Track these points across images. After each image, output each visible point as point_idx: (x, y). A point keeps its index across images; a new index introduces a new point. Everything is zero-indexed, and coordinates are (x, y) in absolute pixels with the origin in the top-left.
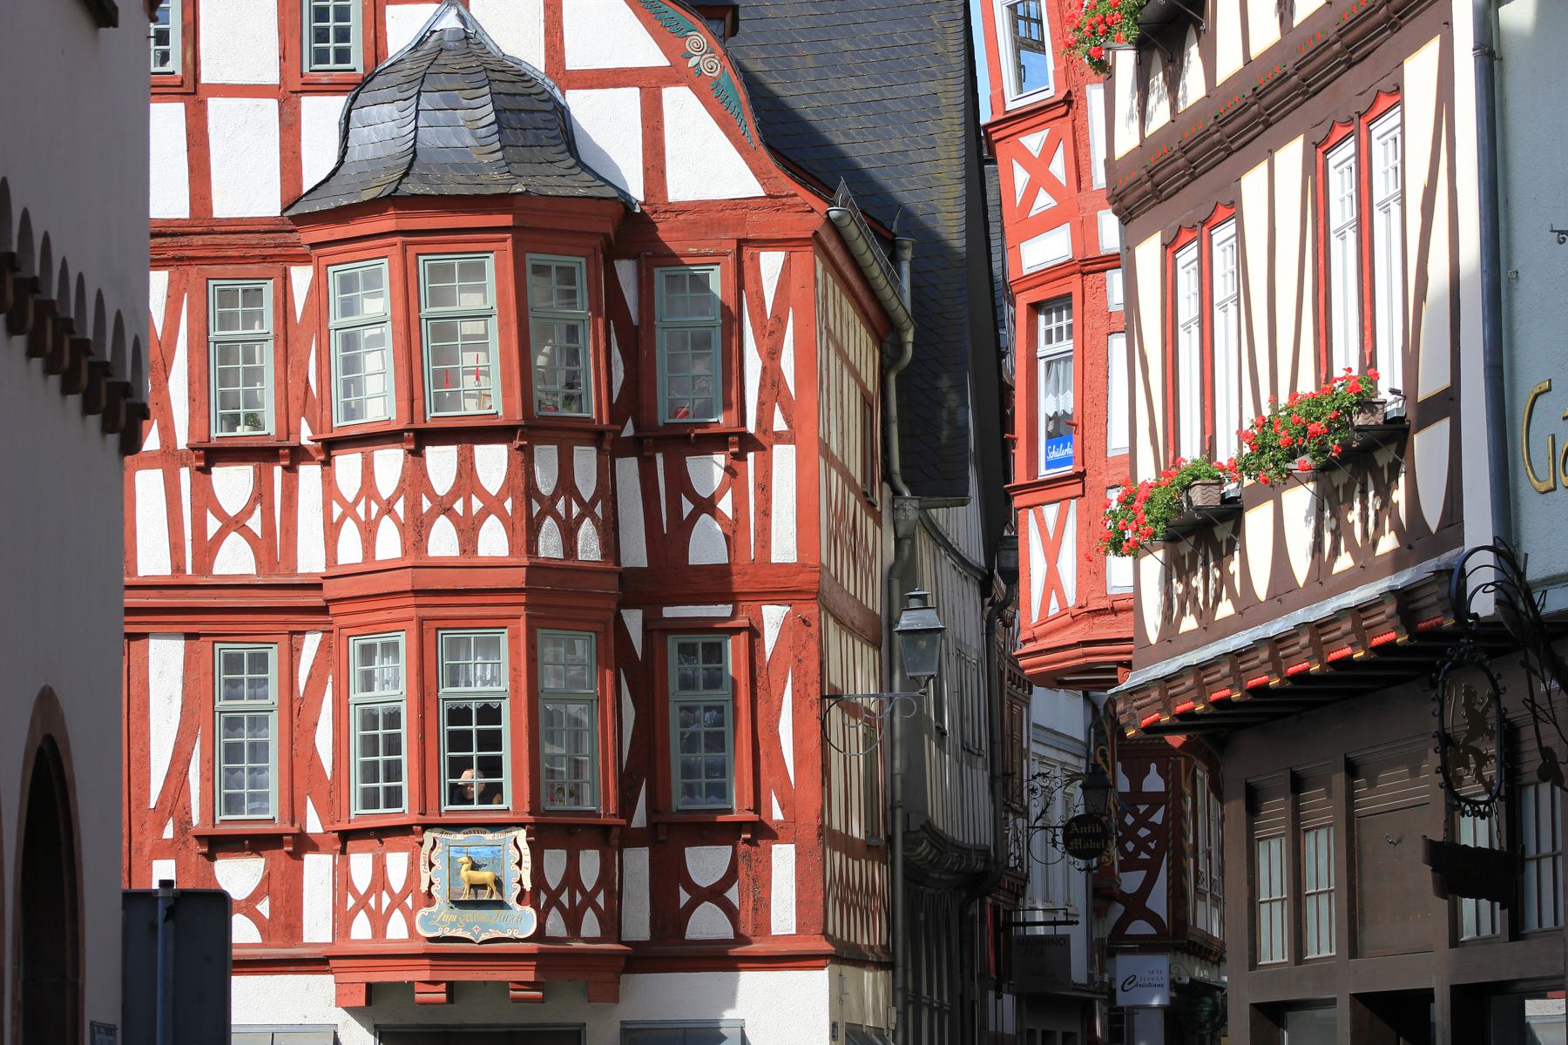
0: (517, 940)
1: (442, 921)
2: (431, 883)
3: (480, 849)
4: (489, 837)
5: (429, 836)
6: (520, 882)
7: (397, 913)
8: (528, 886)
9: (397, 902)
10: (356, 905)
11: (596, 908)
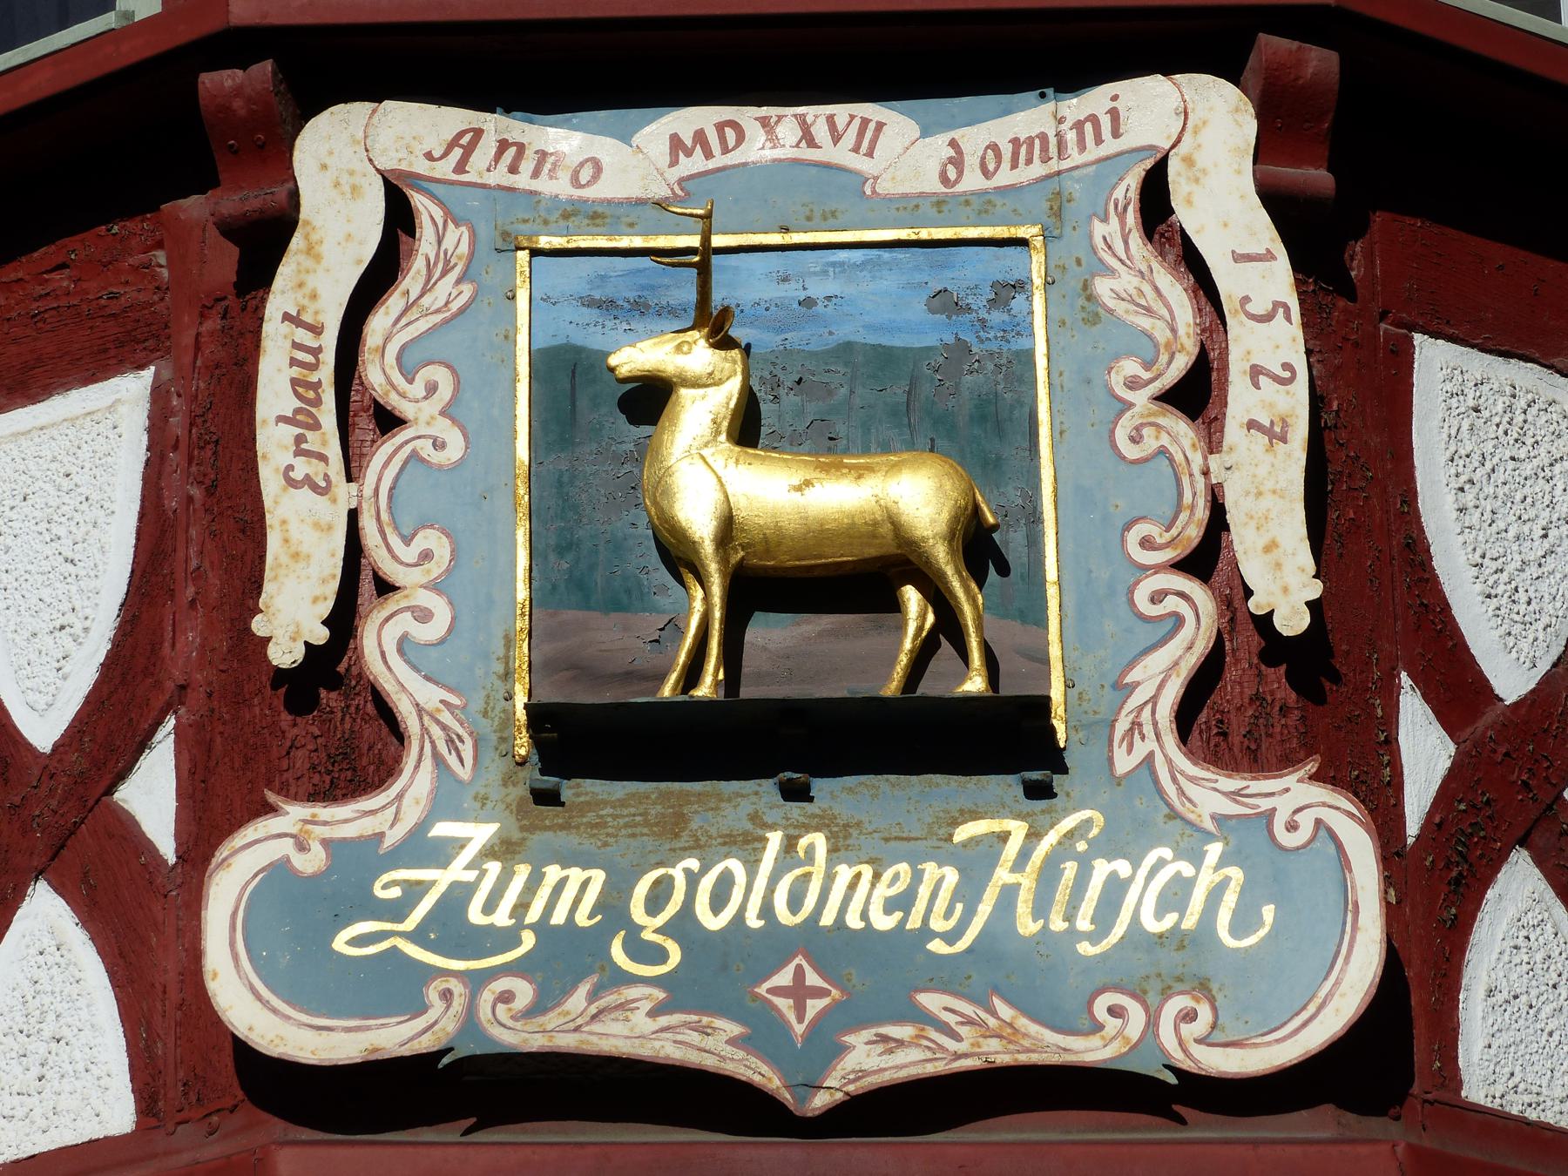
2: (358, 585)
5: (342, 160)
8: (1283, 579)
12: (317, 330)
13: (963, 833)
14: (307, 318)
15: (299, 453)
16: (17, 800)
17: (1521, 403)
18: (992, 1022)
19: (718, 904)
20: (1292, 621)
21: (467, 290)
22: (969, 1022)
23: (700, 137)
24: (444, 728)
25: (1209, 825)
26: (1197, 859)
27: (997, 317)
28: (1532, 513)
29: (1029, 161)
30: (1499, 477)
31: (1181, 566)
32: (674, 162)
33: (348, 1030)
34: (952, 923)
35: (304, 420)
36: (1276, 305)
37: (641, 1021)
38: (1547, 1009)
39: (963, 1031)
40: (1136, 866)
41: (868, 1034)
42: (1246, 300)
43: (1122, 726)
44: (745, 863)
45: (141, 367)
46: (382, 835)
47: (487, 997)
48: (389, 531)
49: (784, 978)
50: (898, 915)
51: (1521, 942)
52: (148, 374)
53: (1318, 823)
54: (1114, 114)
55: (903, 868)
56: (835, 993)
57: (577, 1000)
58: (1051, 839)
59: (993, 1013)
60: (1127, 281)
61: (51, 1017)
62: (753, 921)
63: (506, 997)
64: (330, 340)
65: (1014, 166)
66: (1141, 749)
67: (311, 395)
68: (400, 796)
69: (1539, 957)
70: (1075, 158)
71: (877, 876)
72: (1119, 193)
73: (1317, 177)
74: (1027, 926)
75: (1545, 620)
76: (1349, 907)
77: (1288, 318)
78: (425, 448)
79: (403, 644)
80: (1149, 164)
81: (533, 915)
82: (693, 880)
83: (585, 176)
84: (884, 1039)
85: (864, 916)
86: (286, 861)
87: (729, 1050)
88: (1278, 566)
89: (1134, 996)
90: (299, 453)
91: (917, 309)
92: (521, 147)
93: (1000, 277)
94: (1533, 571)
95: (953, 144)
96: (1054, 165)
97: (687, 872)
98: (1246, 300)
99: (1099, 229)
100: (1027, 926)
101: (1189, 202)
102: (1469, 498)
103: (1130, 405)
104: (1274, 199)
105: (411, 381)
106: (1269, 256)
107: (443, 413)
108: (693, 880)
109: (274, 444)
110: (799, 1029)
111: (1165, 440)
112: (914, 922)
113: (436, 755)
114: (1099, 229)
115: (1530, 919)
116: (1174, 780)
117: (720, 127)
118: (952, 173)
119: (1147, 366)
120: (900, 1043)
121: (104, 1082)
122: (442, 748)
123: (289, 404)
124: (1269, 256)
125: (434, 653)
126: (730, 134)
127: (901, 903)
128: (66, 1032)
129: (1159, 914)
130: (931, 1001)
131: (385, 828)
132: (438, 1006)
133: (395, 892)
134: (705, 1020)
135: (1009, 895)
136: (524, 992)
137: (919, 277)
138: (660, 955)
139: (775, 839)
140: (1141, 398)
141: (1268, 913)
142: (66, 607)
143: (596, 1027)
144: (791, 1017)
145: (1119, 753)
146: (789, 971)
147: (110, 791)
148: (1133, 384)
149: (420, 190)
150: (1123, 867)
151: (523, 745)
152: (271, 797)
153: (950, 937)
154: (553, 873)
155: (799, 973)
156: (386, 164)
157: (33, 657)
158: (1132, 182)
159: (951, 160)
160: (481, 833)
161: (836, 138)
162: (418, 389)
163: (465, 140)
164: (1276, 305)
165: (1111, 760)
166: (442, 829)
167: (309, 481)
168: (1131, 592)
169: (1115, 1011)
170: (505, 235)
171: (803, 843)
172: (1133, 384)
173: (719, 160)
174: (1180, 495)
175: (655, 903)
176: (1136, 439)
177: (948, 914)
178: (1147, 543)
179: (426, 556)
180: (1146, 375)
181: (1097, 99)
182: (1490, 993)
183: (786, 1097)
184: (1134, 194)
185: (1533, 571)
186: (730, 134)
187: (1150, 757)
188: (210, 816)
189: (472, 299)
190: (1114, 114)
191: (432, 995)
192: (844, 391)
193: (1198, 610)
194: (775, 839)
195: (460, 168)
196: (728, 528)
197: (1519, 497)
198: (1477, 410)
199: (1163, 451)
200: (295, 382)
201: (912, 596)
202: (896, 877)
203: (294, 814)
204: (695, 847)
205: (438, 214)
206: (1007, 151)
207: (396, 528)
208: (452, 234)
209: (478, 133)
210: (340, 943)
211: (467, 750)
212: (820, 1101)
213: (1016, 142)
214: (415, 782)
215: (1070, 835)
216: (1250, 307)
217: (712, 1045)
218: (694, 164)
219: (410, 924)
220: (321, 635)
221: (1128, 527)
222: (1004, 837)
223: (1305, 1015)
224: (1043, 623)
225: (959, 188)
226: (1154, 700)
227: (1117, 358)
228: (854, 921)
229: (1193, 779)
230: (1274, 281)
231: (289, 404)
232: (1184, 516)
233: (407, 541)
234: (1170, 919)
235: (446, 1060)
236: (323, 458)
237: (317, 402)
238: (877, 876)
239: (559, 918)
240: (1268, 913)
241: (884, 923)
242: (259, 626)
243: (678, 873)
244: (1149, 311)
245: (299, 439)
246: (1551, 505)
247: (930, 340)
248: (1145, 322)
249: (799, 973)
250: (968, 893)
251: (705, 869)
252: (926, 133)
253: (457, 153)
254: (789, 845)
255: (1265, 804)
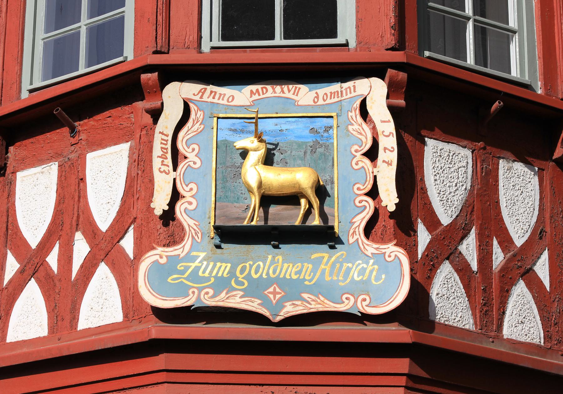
0: (364, 318)
1: (195, 272)
2: (176, 196)
3: (284, 125)
4: (305, 95)
6: (373, 193)
7: (103, 271)
8: (390, 198)
9: (105, 248)
10: (21, 272)
11: (534, 284)
12: (167, 136)
13: (313, 257)
14: (165, 133)
15: (162, 165)
16: (97, 243)
17: (451, 154)
18: (319, 301)
19: (256, 273)
20: (392, 208)
21: (202, 126)
22: (313, 301)
23: (257, 90)
24: (195, 230)
25: (370, 255)
26: (367, 263)
27: (326, 134)
28: (453, 180)
29: (334, 98)
30: (445, 172)
31: (367, 194)
32: (251, 97)
33: (170, 300)
34: (310, 277)
35: (163, 157)
36: (390, 133)
37: (238, 299)
38: (451, 298)
39: (312, 303)
40: (353, 265)
41: (290, 303)
42: (383, 132)
43: (351, 231)
44: (263, 262)
45: (127, 142)
46: (180, 255)
47: (203, 293)
48: (183, 183)
49: (271, 290)
50: (298, 275)
51: (446, 282)
52: (129, 144)
53: (396, 255)
54: (354, 87)
55: (299, 264)
56: (283, 294)
57: (223, 294)
58: (333, 259)
59: (319, 298)
60: (356, 127)
61: (104, 294)
62: (264, 276)
63: (207, 293)
64: (170, 138)
65: (331, 99)
66: (356, 237)
67: (165, 151)
68: (184, 246)
69: (450, 286)
70: (345, 97)
71: (293, 266)
72: (355, 106)
73: (401, 102)
74: (328, 278)
75: (455, 206)
76: (402, 275)
77: (393, 136)
78: (191, 164)
79: (186, 209)
80: (362, 99)
81: (214, 274)
82: (251, 266)
83: (230, 100)
84: (294, 304)
85: (290, 275)
86: (157, 260)
87: (258, 307)
88: (389, 195)
89: (351, 295)
90: (162, 165)
91: (306, 132)
92: (216, 93)
93: (326, 125)
94: (453, 194)
95: (316, 93)
96: (340, 99)
97: (250, 264)
98: (383, 132)
99: (350, 114)
100: (328, 278)
101: (371, 108)
102: (437, 178)
103: (355, 156)
104: (391, 108)
105: (189, 148)
106: (389, 121)
107: (196, 156)
108: (251, 266)
109: (157, 163)
110: (274, 302)
111: (363, 164)
112: (301, 277)
113: (193, 237)
114: (350, 114)
115: (448, 277)
116: (363, 245)
117: (262, 88)
118: (316, 100)
119: (360, 147)
120: (297, 305)
121: (116, 309)
122: (194, 235)
123: (160, 153)
124: (389, 121)
125: (192, 212)
126: (264, 90)
127: (299, 273)
128: (108, 298)
129: (358, 276)
130: (305, 296)
131: (180, 253)
132: (192, 295)
133: (182, 268)
134: (253, 299)
135: (324, 271)
136: (211, 292)
137: (308, 125)
138: (243, 284)
139: (270, 257)
140: (358, 154)
141: (383, 276)
142: (109, 198)
143: (228, 301)
144: (272, 299)
145: (350, 238)
146: (273, 288)
147: (118, 242)
148: (356, 151)
149: (191, 102)
150: (350, 265)
151: (212, 234)
152: (155, 246)
153: (310, 281)
154: (219, 264)
155: (275, 289)
156: (184, 96)
157: (102, 209)
158: (358, 103)
159: (316, 97)
160: (202, 255)
161: (289, 91)
162: (190, 150)
163: (202, 91)
164: (390, 133)
165: (348, 240)
166: (194, 253)
167: (164, 171)
168: (354, 201)
169: (347, 298)
170: (212, 113)
171: (277, 258)
172: (356, 151)
173: (262, 96)
174: (367, 178)
175: (242, 272)
176: (357, 164)
177: (310, 275)
178: (359, 189)
179: (191, 189)
180: (360, 149)
181: (350, 84)
182: (437, 294)
183: (270, 317)
184: (358, 106)
185: (453, 194)
186: (264, 90)
187: (358, 239)
188: (141, 249)
189: (203, 128)
190: (354, 87)
191: (190, 292)
192: (289, 152)
193: (370, 204)
194: (270, 257)
195: (201, 97)
196: (260, 185)
197: (450, 176)
198: (441, 156)
199: (363, 167)
200: (162, 148)
201: (303, 201)
202: (298, 267)
203: (160, 250)
204: (252, 259)
205: (196, 108)
206: (329, 95)
207: (184, 183)
208: (199, 113)
209: (206, 89)
210: (169, 280)
211: (200, 235)
212: (278, 319)
213: (331, 93)
214: (187, 243)
215: (338, 257)
216: (385, 134)
217: (253, 305)
218: (256, 97)
219: (186, 275)
220: (166, 208)
221: (354, 185)
222: (323, 257)
223: (391, 300)
224: (334, 207)
225: (318, 104)
226: (359, 226)
227: (353, 145)
228: (288, 277)
229: (367, 245)
230: (390, 127)
231: (160, 153)
232: (367, 183)
233: (187, 186)
234: (361, 278)
235: (193, 308)
236: (168, 166)
237: (167, 153)
238: (293, 266)
239: (220, 275)
240: (383, 276)
241: (294, 277)
242: (152, 205)
243: (247, 265)
244: (361, 134)
245: (163, 161)
246: (458, 178)
247: (310, 140)
248: (360, 136)
249: (275, 289)
250: (314, 271)
251: (254, 264)
252: (310, 91)
253: (201, 94)
254: (274, 257)
255: (384, 251)
